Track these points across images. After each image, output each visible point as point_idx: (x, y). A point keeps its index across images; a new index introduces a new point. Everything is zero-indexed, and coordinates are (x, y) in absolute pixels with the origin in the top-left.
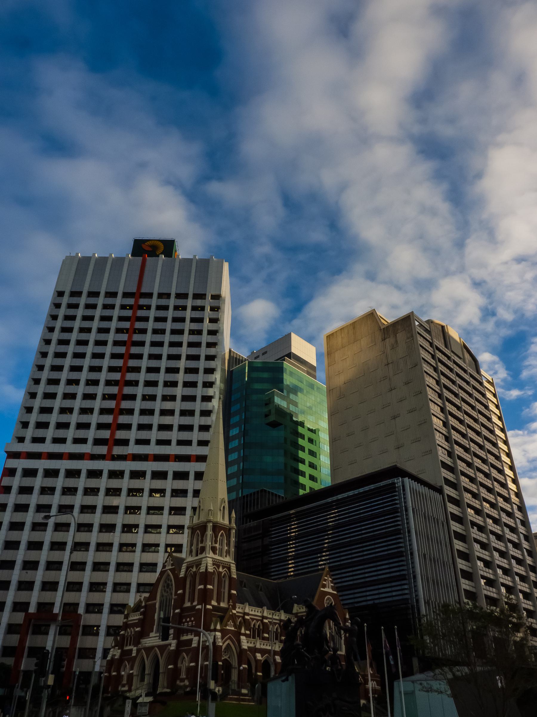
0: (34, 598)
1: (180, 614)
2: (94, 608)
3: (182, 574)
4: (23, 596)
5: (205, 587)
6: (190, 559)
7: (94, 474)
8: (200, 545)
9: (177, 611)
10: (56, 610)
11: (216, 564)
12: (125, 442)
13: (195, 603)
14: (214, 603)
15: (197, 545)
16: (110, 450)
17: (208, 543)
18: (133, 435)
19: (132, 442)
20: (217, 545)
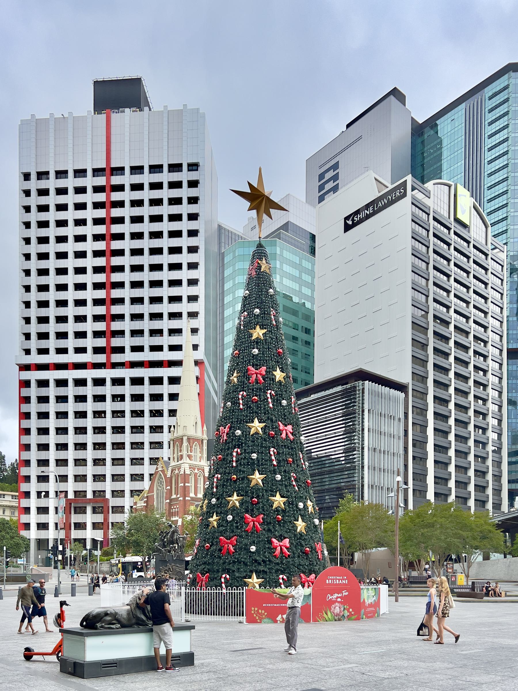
0: (71, 487)
1: (169, 503)
2: (118, 494)
3: (169, 475)
4: (62, 486)
5: (184, 484)
6: (172, 463)
7: (99, 382)
8: (180, 454)
9: (168, 501)
10: (90, 495)
11: (192, 467)
12: (121, 350)
13: (179, 496)
14: (192, 495)
15: (178, 453)
16: (108, 358)
17: (184, 453)
18: (127, 342)
19: (128, 349)
20: (192, 454)
